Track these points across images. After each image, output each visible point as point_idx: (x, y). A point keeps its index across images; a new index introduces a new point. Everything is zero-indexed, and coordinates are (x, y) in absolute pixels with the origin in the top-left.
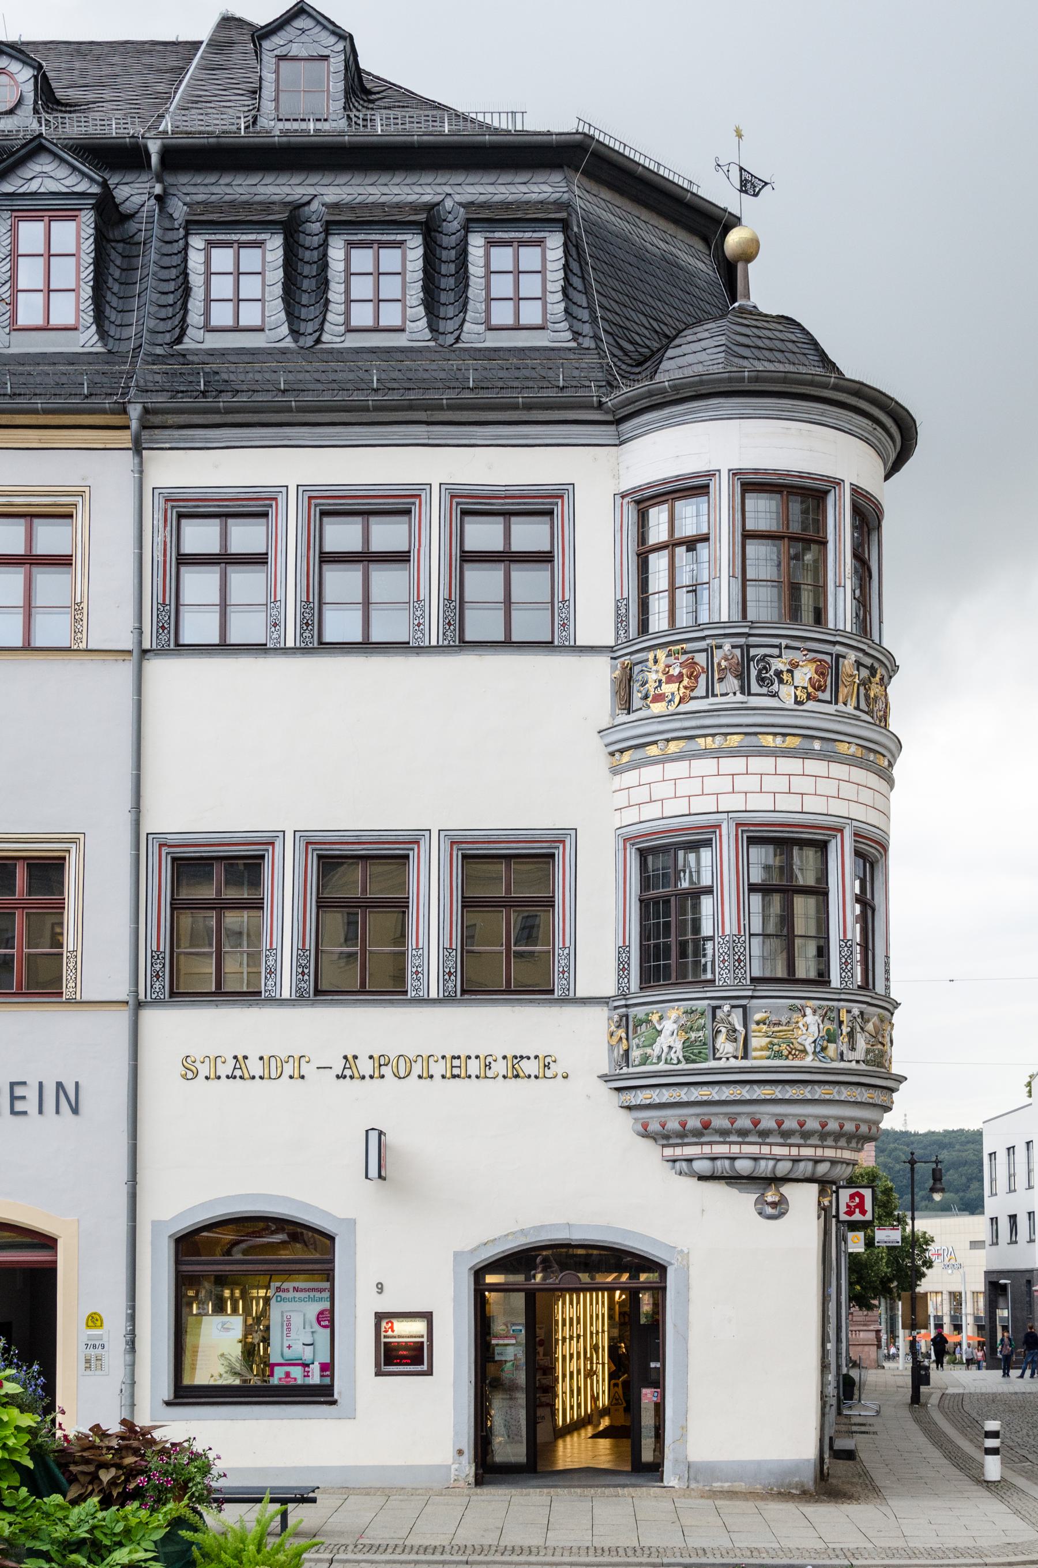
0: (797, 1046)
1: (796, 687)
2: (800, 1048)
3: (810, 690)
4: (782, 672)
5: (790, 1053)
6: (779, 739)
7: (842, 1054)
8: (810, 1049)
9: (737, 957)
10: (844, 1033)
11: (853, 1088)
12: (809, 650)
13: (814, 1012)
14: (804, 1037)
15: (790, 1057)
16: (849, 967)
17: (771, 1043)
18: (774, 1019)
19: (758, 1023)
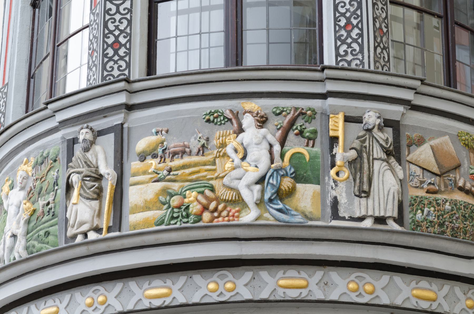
0: (222, 192)
2: (229, 195)
5: (205, 208)
7: (335, 203)
8: (250, 195)
9: (111, 40)
10: (339, 162)
11: (367, 275)
13: (262, 121)
14: (235, 173)
15: (206, 216)
16: (356, 31)
17: (165, 191)
18: (173, 143)
19: (143, 157)
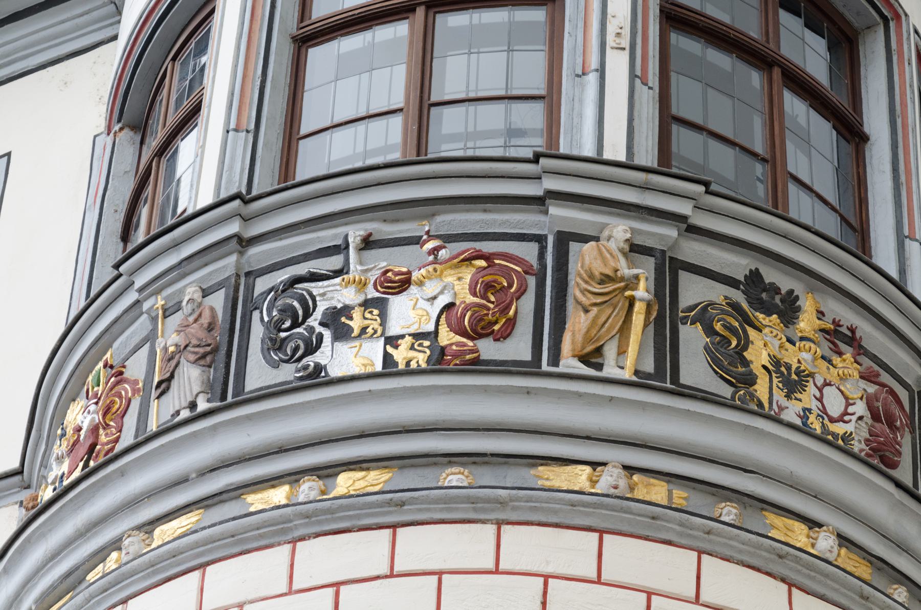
1: (393, 341)
3: (446, 337)
4: (346, 310)
6: (308, 489)
12: (449, 239)
